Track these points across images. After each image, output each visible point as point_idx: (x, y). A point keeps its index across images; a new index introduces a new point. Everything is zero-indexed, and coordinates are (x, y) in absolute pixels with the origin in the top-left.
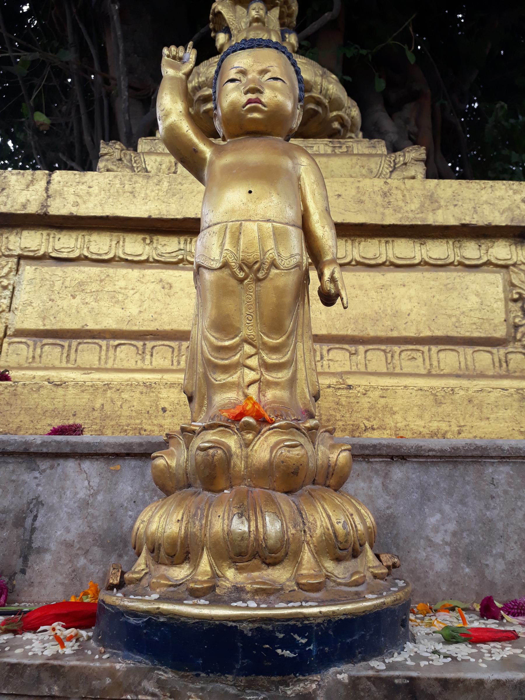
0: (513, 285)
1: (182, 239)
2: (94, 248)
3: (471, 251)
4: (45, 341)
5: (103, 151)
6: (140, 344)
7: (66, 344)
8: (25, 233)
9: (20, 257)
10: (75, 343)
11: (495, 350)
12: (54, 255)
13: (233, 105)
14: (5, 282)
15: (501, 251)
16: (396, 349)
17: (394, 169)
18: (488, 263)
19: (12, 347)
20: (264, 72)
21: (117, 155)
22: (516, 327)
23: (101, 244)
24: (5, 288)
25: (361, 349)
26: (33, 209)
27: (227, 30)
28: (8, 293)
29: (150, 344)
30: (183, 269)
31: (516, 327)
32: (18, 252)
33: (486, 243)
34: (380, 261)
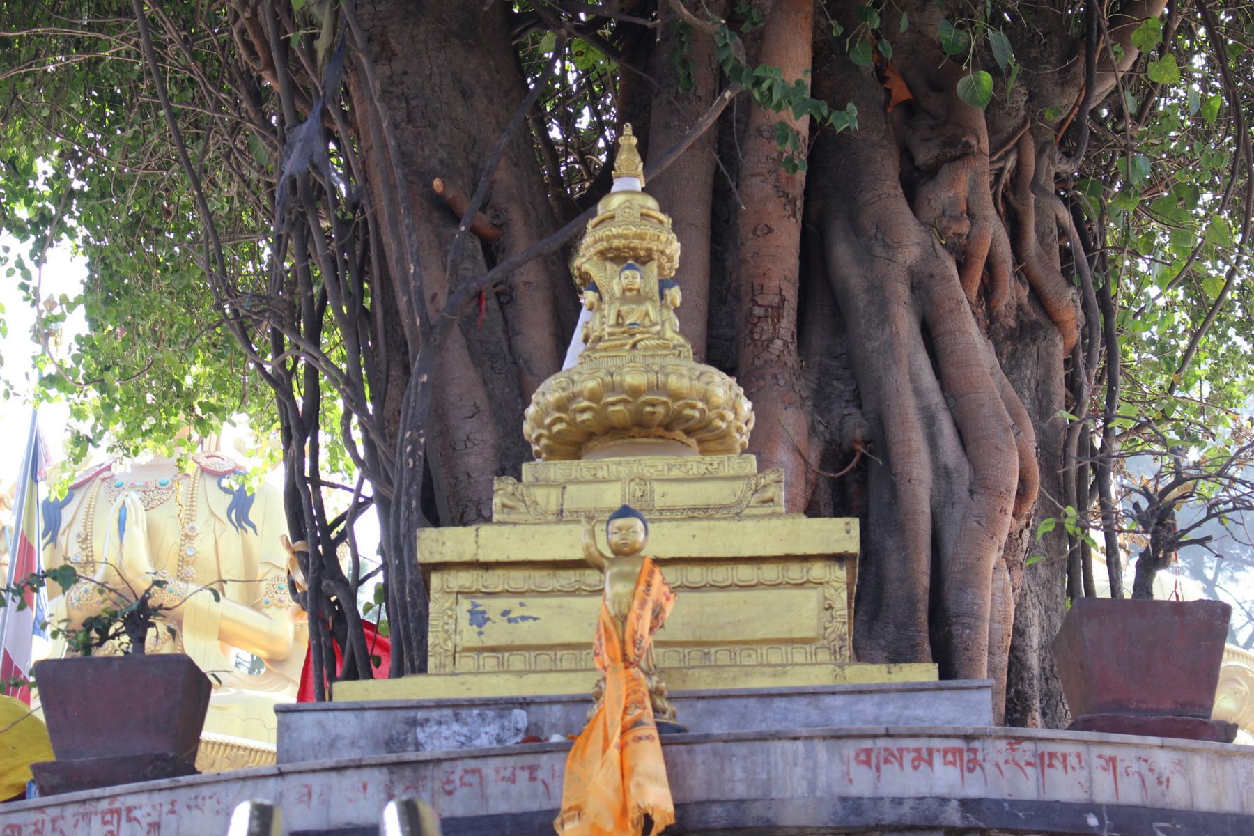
0: (826, 599)
1: (578, 572)
2: (513, 584)
3: (795, 572)
4: (486, 654)
5: (496, 487)
6: (552, 653)
7: (500, 655)
8: (460, 574)
9: (458, 593)
10: (506, 655)
11: (807, 647)
12: (484, 590)
13: (616, 544)
14: (450, 613)
15: (818, 571)
16: (737, 648)
17: (756, 491)
18: (808, 582)
19: (463, 660)
20: (628, 529)
21: (510, 489)
22: (826, 629)
23: (517, 579)
24: (450, 617)
25: (713, 650)
26: (467, 557)
27: (595, 288)
28: (451, 621)
29: (559, 654)
30: (579, 596)
31: (826, 629)
32: (456, 589)
33: (806, 565)
34: (727, 583)
